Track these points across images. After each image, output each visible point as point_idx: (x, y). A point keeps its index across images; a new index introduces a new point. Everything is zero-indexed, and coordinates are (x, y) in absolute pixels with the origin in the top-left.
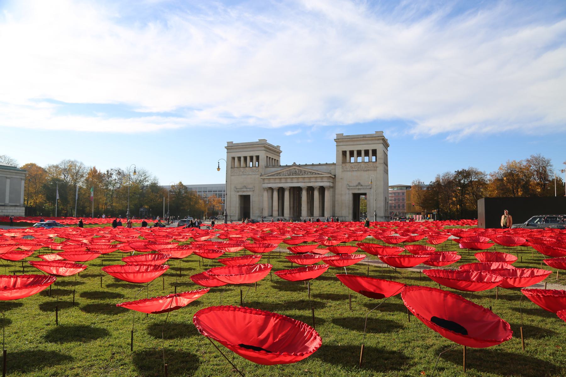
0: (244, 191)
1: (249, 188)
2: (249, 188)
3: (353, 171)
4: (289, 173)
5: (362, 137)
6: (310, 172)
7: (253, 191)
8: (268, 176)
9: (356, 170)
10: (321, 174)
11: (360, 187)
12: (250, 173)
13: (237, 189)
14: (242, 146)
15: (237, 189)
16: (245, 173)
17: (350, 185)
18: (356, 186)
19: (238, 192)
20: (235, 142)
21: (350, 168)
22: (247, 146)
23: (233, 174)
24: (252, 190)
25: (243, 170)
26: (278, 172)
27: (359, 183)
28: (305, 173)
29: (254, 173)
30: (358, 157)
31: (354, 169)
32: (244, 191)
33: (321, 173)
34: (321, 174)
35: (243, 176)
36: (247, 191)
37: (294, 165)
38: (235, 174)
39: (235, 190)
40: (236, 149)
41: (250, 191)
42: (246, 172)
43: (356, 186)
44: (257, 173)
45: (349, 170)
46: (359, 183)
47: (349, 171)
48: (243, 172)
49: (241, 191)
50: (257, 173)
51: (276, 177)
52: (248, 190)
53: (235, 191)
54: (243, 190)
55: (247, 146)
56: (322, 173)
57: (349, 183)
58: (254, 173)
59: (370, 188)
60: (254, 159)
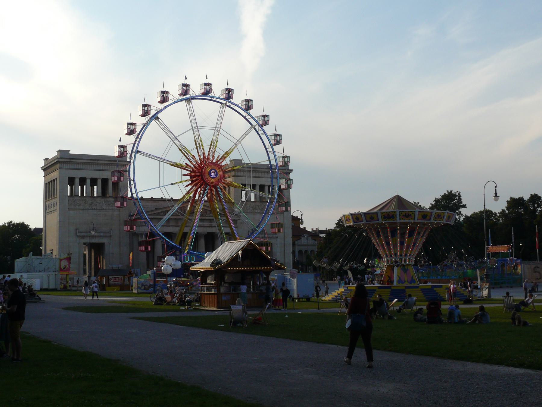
1: (103, 232)
2: (103, 232)
3: (256, 213)
5: (266, 167)
7: (111, 236)
9: (259, 211)
12: (104, 207)
15: (81, 232)
16: (94, 207)
19: (83, 237)
20: (74, 151)
21: (251, 209)
22: (99, 162)
24: (108, 235)
25: (90, 202)
26: (166, 209)
29: (111, 208)
30: (498, 196)
36: (99, 236)
39: (78, 234)
40: (78, 163)
41: (106, 237)
42: (96, 205)
47: (252, 213)
48: (91, 205)
49: (87, 236)
52: (102, 234)
53: (78, 236)
55: (99, 162)
58: (111, 208)
59: (277, 237)
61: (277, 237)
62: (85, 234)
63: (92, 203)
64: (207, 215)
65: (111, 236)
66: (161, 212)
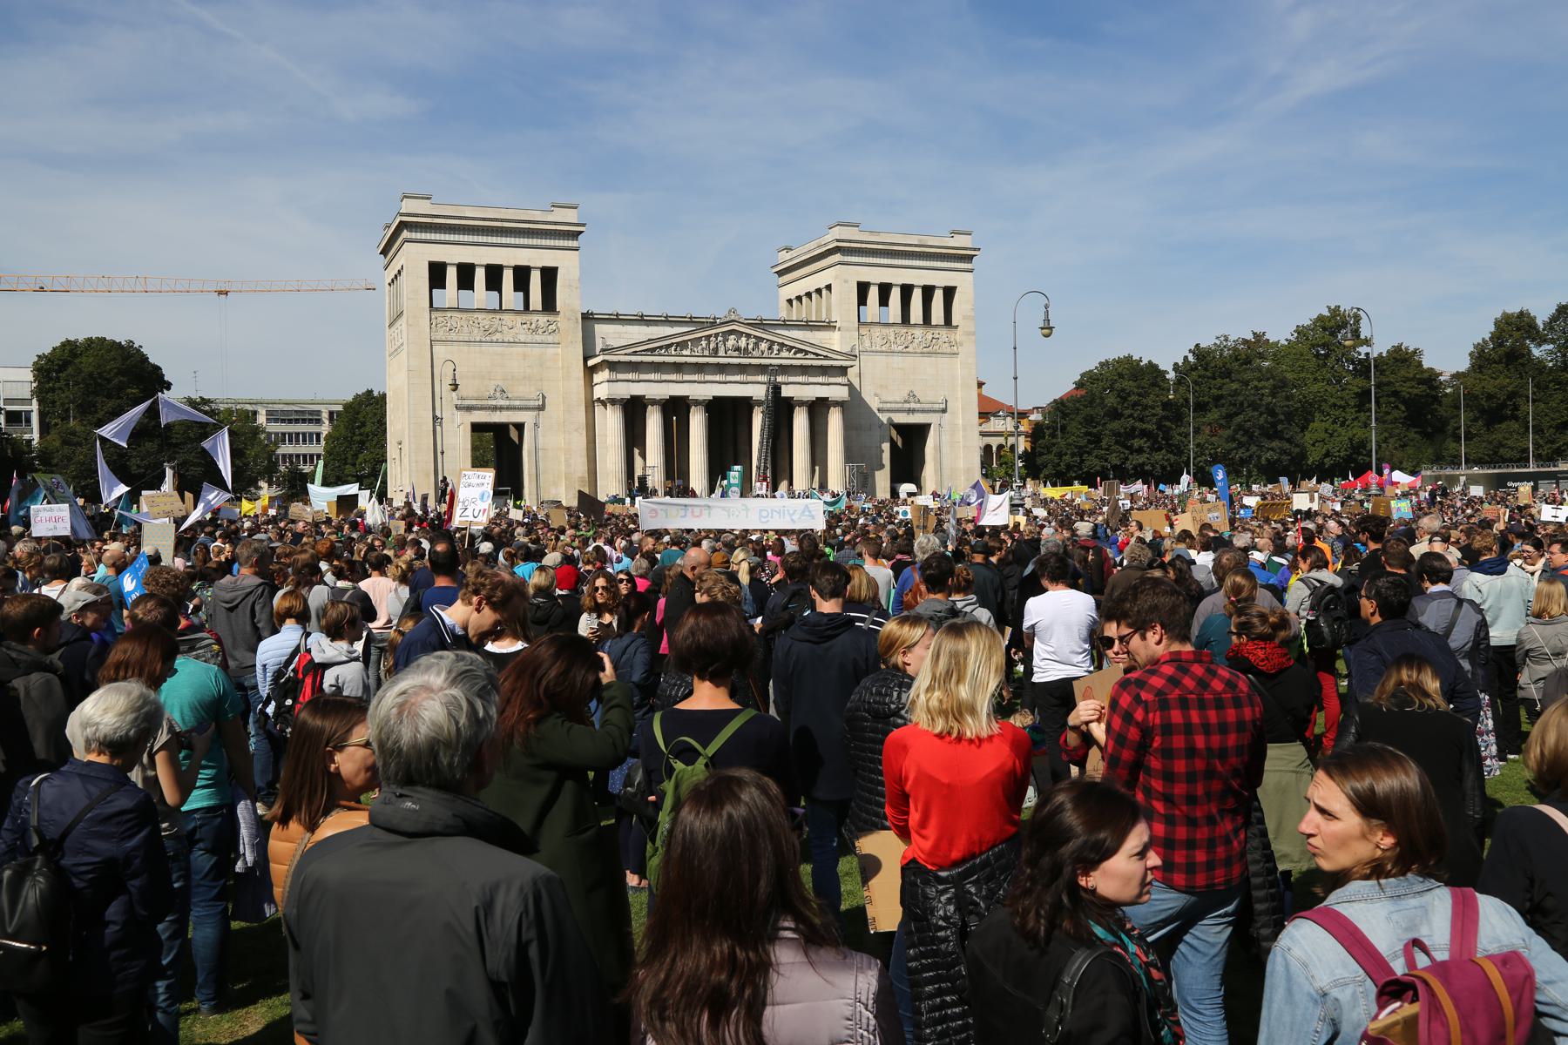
0: (495, 408)
4: (712, 345)
6: (790, 348)
8: (635, 353)
9: (900, 348)
10: (826, 358)
11: (913, 406)
13: (462, 399)
14: (484, 219)
15: (462, 399)
16: (498, 336)
17: (885, 398)
18: (905, 402)
19: (469, 409)
23: (440, 335)
24: (532, 403)
27: (912, 395)
28: (770, 348)
29: (538, 338)
31: (894, 347)
32: (495, 408)
33: (825, 354)
34: (826, 358)
35: (486, 348)
36: (508, 408)
37: (733, 318)
38: (453, 336)
39: (459, 402)
43: (905, 402)
44: (550, 339)
45: (878, 348)
46: (912, 395)
50: (550, 339)
51: (667, 359)
52: (517, 403)
54: (494, 402)
56: (829, 355)
57: (878, 392)
58: (538, 338)
60: (508, 278)
61: (944, 411)
62: (474, 402)
63: (490, 327)
64: (773, 356)
65: (542, 408)
66: (661, 348)
